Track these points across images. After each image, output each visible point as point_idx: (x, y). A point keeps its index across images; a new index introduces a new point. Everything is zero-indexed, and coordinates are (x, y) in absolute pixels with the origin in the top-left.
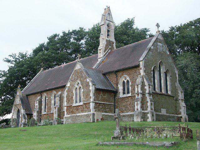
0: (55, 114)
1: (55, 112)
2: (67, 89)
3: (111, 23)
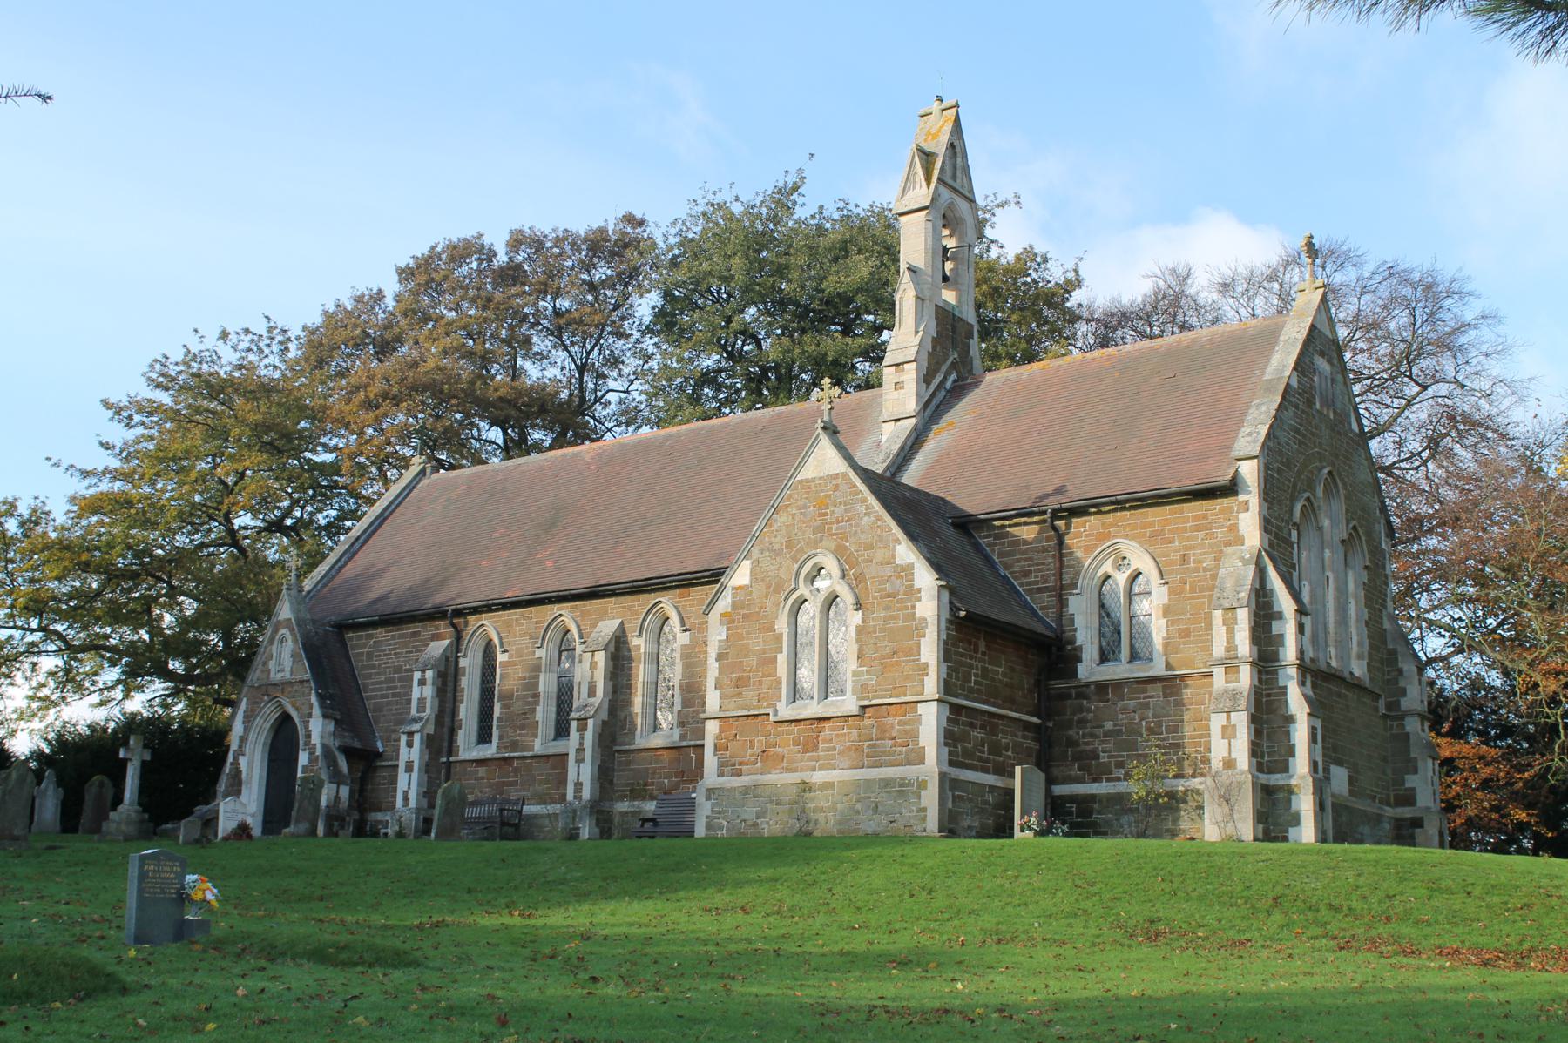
0: (579, 761)
1: (581, 750)
2: (725, 603)
3: (963, 205)
